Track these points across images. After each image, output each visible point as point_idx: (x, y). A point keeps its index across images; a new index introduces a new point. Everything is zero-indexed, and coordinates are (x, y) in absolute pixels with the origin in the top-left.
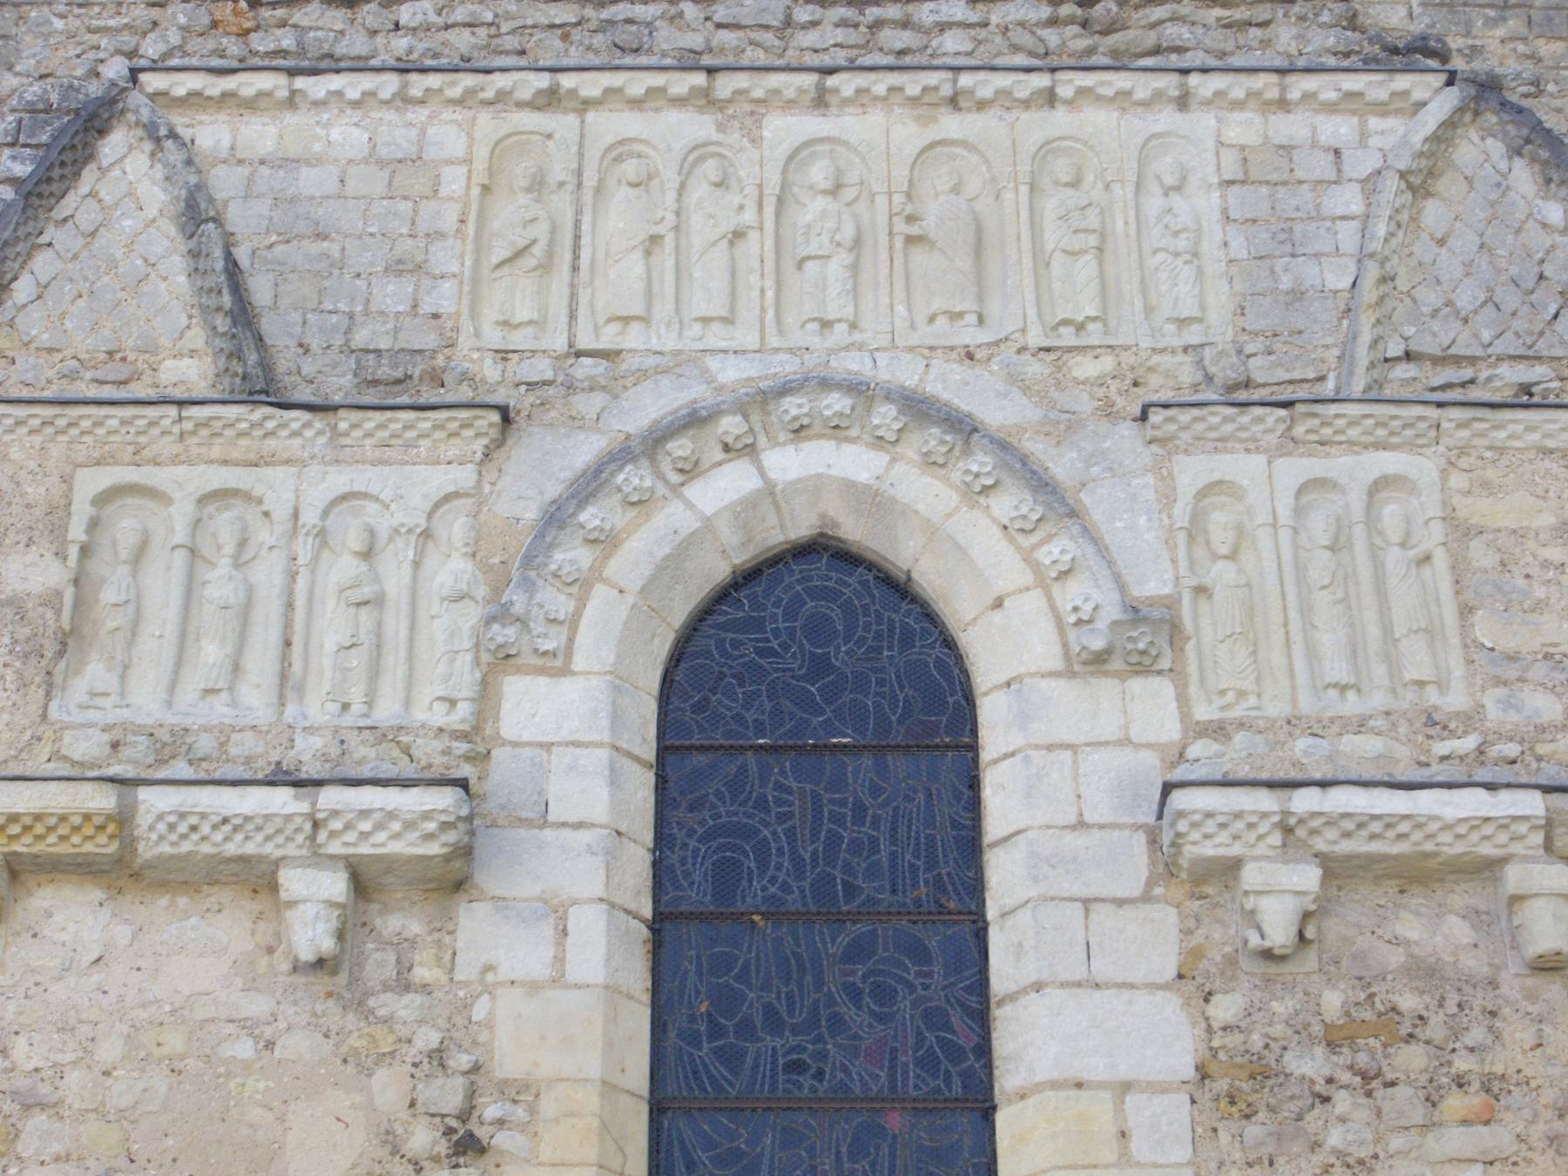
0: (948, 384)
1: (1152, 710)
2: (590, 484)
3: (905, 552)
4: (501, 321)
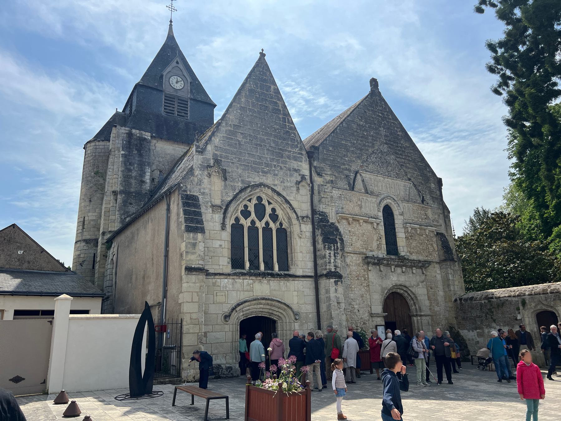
0: (394, 197)
1: (402, 217)
2: (381, 200)
3: (392, 208)
4: (375, 189)
